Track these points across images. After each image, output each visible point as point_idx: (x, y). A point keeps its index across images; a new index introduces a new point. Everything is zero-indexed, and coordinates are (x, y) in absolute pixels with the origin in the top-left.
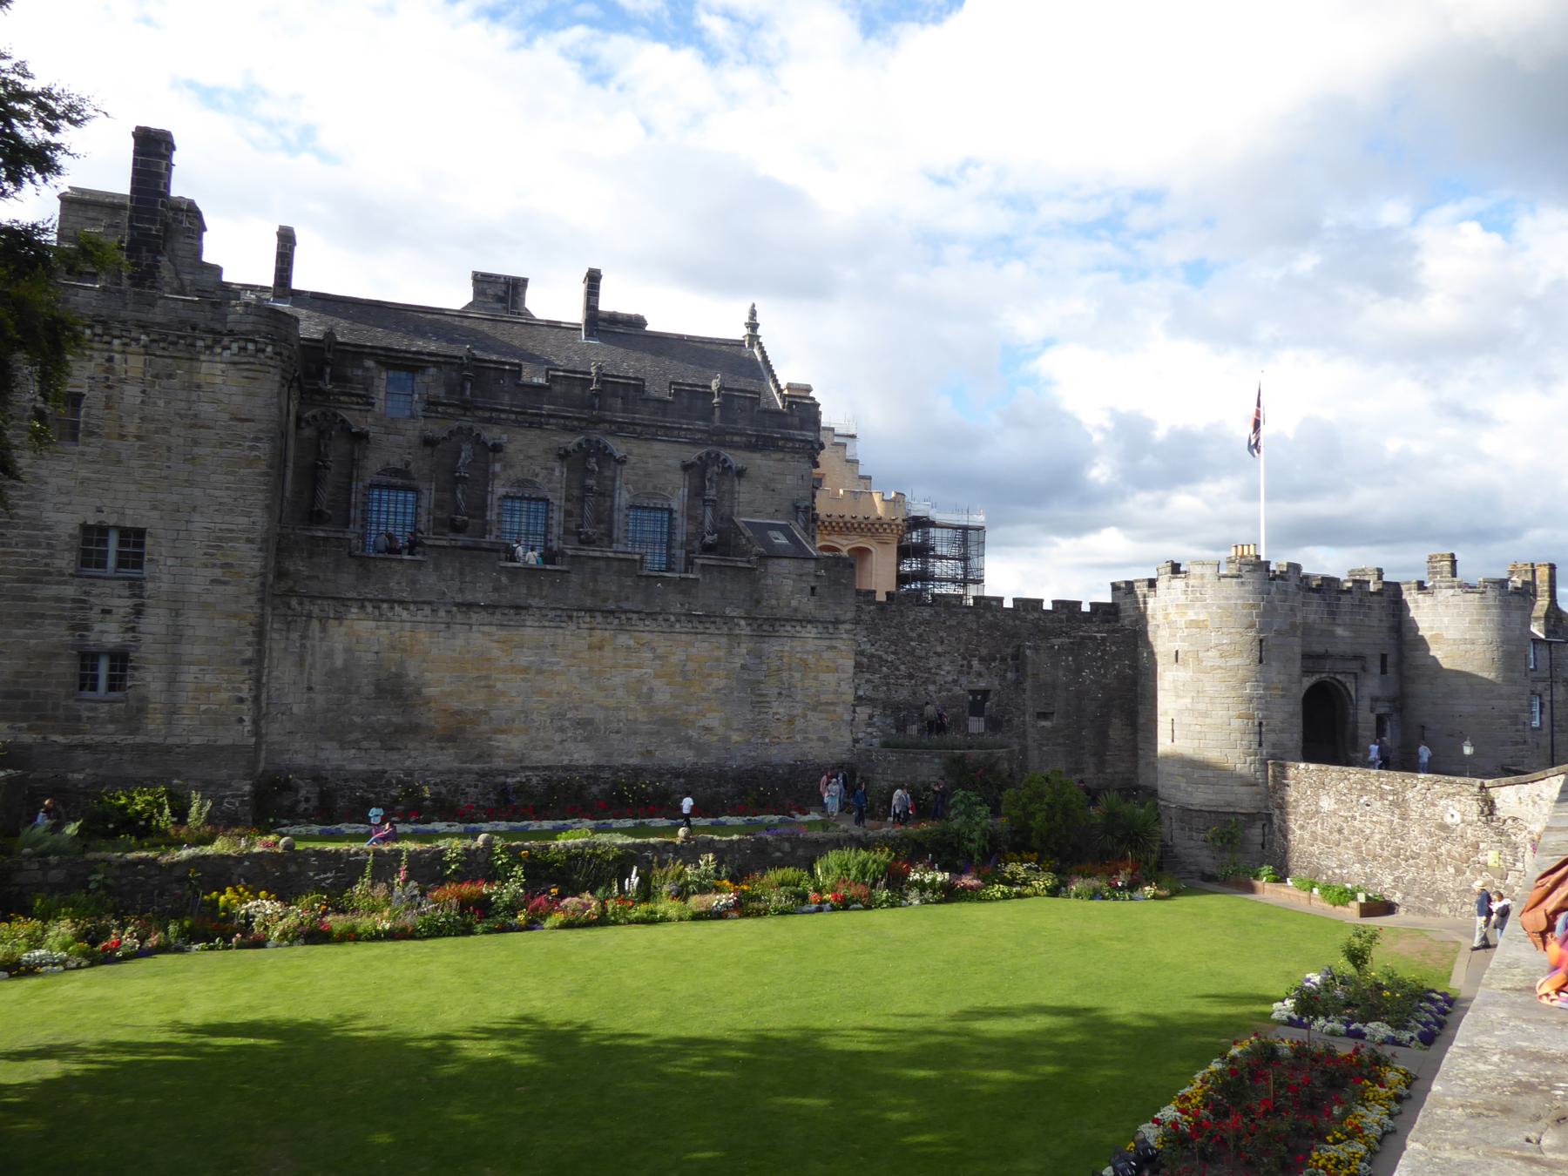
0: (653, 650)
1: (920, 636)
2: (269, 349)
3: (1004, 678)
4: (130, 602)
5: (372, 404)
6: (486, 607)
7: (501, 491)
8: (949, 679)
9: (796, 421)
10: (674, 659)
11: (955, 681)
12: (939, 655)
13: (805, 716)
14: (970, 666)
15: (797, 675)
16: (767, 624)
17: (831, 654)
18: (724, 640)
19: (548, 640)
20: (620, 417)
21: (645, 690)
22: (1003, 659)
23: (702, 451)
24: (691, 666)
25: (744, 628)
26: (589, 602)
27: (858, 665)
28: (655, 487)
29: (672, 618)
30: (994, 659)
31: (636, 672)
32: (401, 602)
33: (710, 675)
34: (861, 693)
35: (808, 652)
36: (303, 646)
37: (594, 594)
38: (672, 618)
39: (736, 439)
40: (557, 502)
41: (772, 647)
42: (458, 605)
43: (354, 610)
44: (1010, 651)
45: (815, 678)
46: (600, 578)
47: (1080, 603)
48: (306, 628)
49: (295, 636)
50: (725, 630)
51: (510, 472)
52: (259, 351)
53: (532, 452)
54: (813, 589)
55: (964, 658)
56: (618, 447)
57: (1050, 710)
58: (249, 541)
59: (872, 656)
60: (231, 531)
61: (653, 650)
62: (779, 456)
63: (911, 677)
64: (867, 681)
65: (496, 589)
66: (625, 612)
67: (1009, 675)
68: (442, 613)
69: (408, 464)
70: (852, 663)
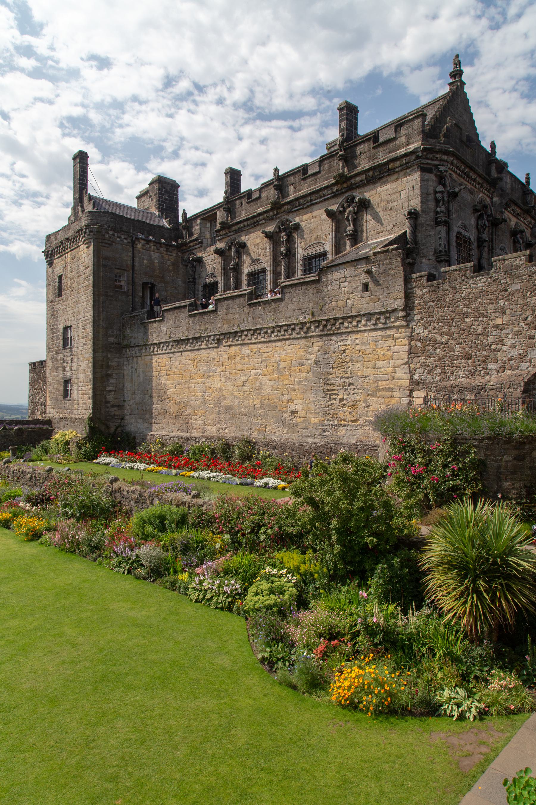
1: (476, 310)
2: (87, 231)
4: (69, 358)
8: (514, 353)
10: (273, 360)
11: (522, 357)
13: (366, 401)
15: (358, 365)
17: (388, 343)
18: (303, 342)
21: (257, 385)
23: (341, 199)
25: (314, 331)
28: (316, 239)
29: (269, 331)
34: (416, 377)
37: (228, 322)
38: (269, 331)
39: (358, 179)
40: (268, 269)
43: (144, 351)
46: (230, 311)
49: (130, 367)
50: (302, 334)
52: (85, 233)
53: (258, 241)
58: (89, 323)
60: (86, 320)
61: (261, 355)
66: (243, 331)
70: (407, 348)
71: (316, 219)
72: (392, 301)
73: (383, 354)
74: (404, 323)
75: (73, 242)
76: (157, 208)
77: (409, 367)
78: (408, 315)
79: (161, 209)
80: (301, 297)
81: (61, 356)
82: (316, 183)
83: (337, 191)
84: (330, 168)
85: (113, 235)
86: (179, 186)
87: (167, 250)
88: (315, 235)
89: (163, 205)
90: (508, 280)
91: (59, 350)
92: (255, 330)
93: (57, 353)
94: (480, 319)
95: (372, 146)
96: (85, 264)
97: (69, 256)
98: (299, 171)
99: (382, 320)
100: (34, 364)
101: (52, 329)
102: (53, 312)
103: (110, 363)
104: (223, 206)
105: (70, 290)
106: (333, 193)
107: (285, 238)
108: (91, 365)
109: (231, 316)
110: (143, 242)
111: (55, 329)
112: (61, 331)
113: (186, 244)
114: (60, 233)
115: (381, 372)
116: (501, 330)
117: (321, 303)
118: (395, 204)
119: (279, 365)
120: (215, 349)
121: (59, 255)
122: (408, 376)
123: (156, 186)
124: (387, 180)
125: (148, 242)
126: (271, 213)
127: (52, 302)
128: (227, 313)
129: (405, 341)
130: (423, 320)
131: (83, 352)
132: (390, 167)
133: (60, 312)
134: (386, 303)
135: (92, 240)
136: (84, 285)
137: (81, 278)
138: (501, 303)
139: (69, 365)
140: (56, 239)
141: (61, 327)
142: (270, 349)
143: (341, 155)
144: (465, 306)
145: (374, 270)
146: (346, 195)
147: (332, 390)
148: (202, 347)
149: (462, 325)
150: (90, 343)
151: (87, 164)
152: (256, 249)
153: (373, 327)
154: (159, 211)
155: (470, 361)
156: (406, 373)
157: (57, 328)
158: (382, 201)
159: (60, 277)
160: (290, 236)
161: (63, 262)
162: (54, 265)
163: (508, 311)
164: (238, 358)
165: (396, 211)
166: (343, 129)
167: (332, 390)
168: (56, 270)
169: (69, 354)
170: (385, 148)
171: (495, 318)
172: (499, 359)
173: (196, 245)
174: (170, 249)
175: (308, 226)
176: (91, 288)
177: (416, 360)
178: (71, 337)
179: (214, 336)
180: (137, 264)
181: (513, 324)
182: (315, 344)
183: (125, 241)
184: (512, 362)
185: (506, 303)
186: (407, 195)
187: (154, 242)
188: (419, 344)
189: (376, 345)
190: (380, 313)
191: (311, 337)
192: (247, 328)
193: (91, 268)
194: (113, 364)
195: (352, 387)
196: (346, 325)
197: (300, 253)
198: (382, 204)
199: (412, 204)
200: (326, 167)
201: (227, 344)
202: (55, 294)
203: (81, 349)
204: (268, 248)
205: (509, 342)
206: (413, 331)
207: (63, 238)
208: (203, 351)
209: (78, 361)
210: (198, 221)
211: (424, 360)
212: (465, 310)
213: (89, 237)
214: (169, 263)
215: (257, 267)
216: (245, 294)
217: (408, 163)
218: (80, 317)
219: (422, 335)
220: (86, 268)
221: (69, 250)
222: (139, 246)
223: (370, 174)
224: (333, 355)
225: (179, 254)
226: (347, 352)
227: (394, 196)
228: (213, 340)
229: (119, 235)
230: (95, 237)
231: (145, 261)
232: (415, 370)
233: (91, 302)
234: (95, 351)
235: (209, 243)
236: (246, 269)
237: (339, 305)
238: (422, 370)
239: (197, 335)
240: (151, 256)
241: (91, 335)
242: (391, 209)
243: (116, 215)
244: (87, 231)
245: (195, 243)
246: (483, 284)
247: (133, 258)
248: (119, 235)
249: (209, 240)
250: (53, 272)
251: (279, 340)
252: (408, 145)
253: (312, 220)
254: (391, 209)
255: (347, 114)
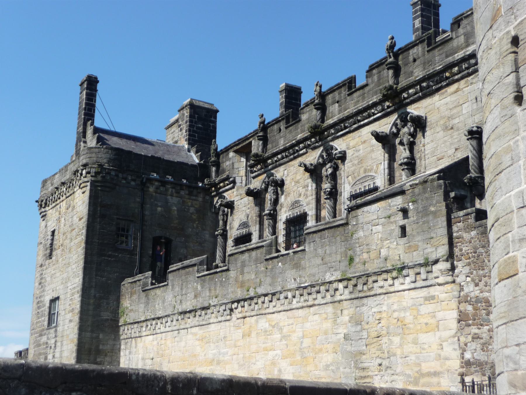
0: (281, 329)
2: (84, 172)
4: (53, 341)
5: (234, 182)
6: (190, 312)
7: (283, 215)
9: (462, 39)
10: (294, 337)
15: (396, 340)
16: (360, 282)
18: (329, 309)
19: (222, 335)
20: (335, 119)
23: (394, 117)
24: (307, 342)
25: (343, 292)
26: (240, 294)
27: (463, 318)
28: (365, 172)
29: (290, 295)
31: (271, 353)
32: (159, 318)
33: (321, 350)
34: (468, 356)
35: (405, 309)
36: (129, 358)
37: (242, 285)
38: (290, 295)
41: (371, 308)
42: (181, 313)
43: (144, 329)
45: (415, 342)
46: (246, 270)
48: (131, 347)
50: (328, 298)
51: (289, 199)
53: (298, 177)
54: (403, 229)
56: (339, 145)
59: (478, 300)
62: (455, 86)
64: (476, 337)
65: (196, 297)
68: (175, 322)
69: (248, 217)
70: (455, 314)
71: (365, 145)
72: (434, 249)
73: (426, 324)
74: (450, 279)
75: (69, 187)
76: (186, 140)
77: (459, 340)
78: (453, 268)
79: (191, 141)
80: (327, 247)
81: (44, 339)
82: (363, 99)
83: (388, 107)
84: (379, 79)
85: (117, 176)
86: (217, 111)
87: (190, 194)
88: (364, 165)
89: (195, 136)
91: (43, 330)
92: (274, 294)
93: (41, 335)
95: (426, 49)
96: (79, 214)
97: (64, 205)
98: (344, 85)
99: (423, 276)
100: (20, 353)
101: (38, 303)
102: (41, 279)
103: (101, 347)
104: (257, 133)
105: (61, 248)
106: (383, 110)
107: (330, 171)
108: (75, 348)
109: (247, 277)
110: (157, 183)
111: (41, 302)
112: (48, 305)
113: (215, 185)
114: (57, 176)
115: (424, 349)
117: (350, 253)
118: (456, 121)
119: (302, 342)
120: (227, 323)
121: (54, 205)
122: (459, 352)
123: (186, 113)
124: (446, 91)
125: (164, 183)
126: (313, 140)
127: (41, 266)
128: (242, 273)
129: (454, 304)
130: (472, 273)
131: (68, 332)
132: (447, 74)
133: (48, 279)
134: (426, 251)
135: (89, 184)
136: (76, 241)
137: (74, 233)
139: (52, 350)
140: (52, 185)
141: (47, 299)
142: (291, 321)
143: (390, 63)
145: (411, 207)
146: (401, 111)
147: (365, 377)
148: (211, 321)
150: (77, 318)
151: (96, 91)
152: (296, 188)
153: (413, 285)
154: (189, 144)
156: (455, 349)
157: (43, 301)
158: (442, 118)
159: (53, 232)
160: (336, 168)
161: (57, 213)
162: (48, 218)
164: (253, 334)
165: (458, 130)
166: (418, 29)
167: (365, 377)
168: (49, 224)
169: (54, 336)
170: (441, 52)
173: (228, 185)
174: (195, 192)
175: (356, 154)
176: (83, 245)
177: (467, 330)
178: (58, 312)
179: (226, 304)
180: (147, 213)
182: (345, 312)
183: (133, 183)
186: (470, 109)
187: (171, 183)
188: (470, 308)
189: (418, 311)
190: (421, 265)
191: (340, 301)
192: (264, 292)
193: (85, 219)
194: (105, 348)
195: (389, 371)
196: (381, 283)
197: (346, 190)
198: (442, 122)
199: (477, 121)
200: (375, 78)
201: (240, 315)
202: (45, 255)
203: (66, 328)
204: (310, 185)
206: (462, 289)
207: (59, 183)
208: (213, 325)
209: (62, 345)
210: (231, 154)
211: (477, 331)
213: (86, 180)
214: (192, 210)
215: (297, 212)
216: (262, 246)
217: (467, 68)
218: (69, 284)
219: (472, 295)
220: (80, 219)
221: (64, 197)
222: (151, 189)
223: (424, 84)
224: (366, 327)
225: (208, 198)
226: (382, 322)
227: (455, 111)
228: (225, 310)
229: (125, 175)
230: (93, 179)
231: (159, 209)
232: (466, 345)
233: (81, 264)
234: (81, 329)
235: (244, 182)
236: (283, 215)
237: (372, 257)
238: (473, 346)
239: (206, 305)
240: (167, 202)
241: (77, 306)
242: (452, 128)
243: (122, 150)
244: (84, 172)
245: (227, 182)
247: (142, 205)
248: (125, 175)
249: (244, 178)
250: (46, 226)
251: (302, 307)
252: (468, 46)
253: (361, 147)
254: (452, 128)
255: (422, 10)
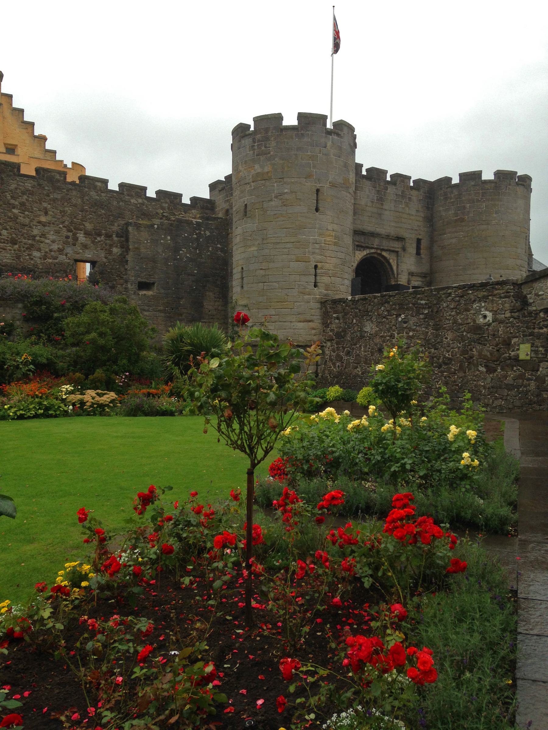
1: (22, 204)
3: (110, 252)
8: (55, 247)
11: (60, 251)
12: (44, 225)
14: (76, 239)
22: (108, 236)
30: (100, 235)
44: (115, 228)
47: (180, 196)
55: (69, 231)
57: (152, 280)
63: (14, 242)
67: (115, 250)
90: (51, 188)
94: (27, 213)
116: (44, 226)
138: (45, 205)
144: (12, 197)
149: (10, 214)
155: (16, 247)
163: (50, 213)
171: (40, 215)
172: (42, 248)
181: (53, 224)
184: (53, 253)
185: (49, 206)
205: (52, 237)
212: (12, 201)
246: (29, 185)
